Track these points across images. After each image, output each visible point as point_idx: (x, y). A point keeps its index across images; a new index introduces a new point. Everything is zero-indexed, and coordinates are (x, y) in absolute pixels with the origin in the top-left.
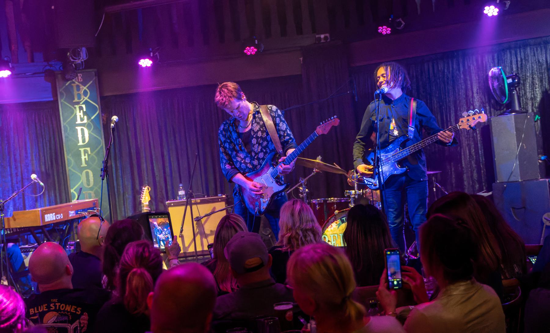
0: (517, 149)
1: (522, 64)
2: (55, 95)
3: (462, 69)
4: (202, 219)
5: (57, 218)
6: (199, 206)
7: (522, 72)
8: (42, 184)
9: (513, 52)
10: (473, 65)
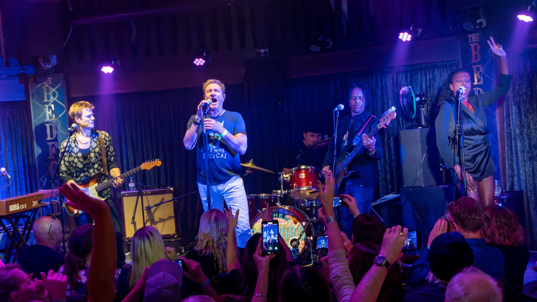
0: (421, 159)
1: (430, 84)
2: (27, 95)
3: (380, 85)
4: (152, 209)
5: (21, 208)
6: (148, 197)
7: (430, 90)
8: (9, 177)
9: (423, 72)
10: (389, 82)
